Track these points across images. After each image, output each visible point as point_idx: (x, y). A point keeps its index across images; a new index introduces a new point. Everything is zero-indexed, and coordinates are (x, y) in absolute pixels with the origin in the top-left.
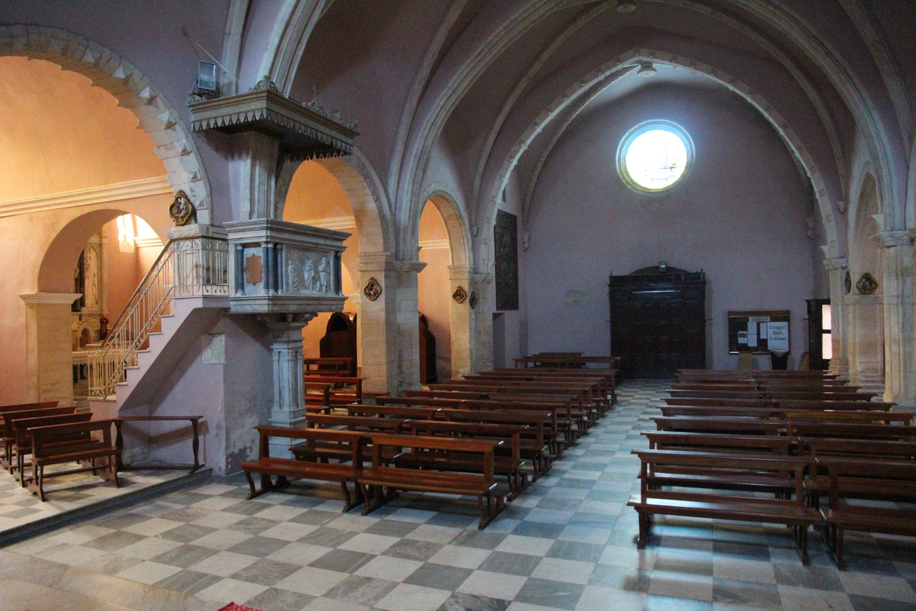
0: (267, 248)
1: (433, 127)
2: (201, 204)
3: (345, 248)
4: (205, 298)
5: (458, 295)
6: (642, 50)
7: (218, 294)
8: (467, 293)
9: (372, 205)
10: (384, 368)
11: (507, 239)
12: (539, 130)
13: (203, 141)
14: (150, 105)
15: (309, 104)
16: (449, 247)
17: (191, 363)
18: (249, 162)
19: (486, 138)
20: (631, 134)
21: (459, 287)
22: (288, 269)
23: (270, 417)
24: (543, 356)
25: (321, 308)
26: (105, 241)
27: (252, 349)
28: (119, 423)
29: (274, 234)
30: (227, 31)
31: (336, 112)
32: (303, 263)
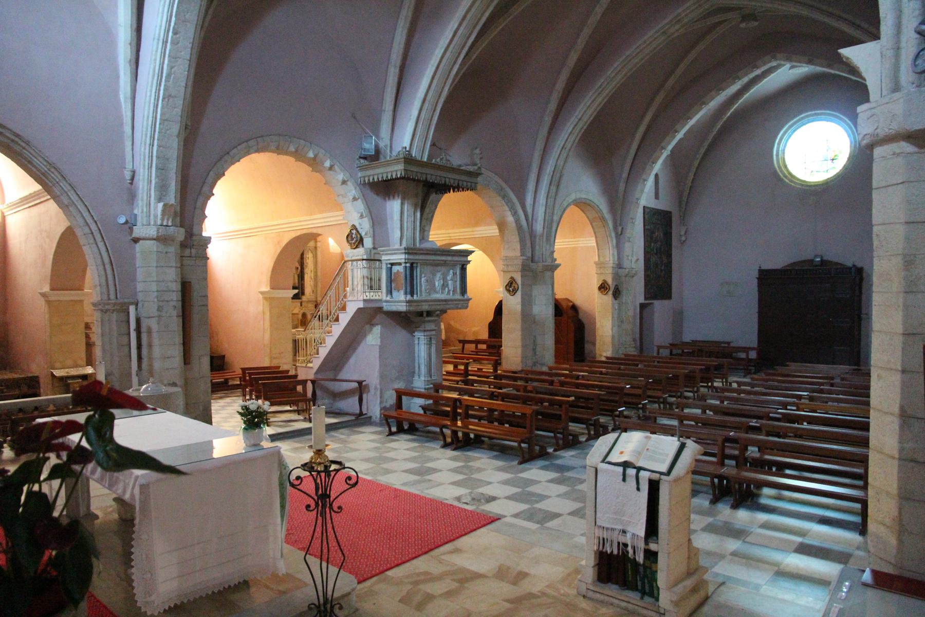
0: (406, 267)
1: (563, 150)
2: (366, 234)
3: (469, 262)
4: (365, 301)
5: (603, 287)
6: (778, 55)
7: (374, 298)
8: (611, 286)
9: (510, 219)
10: (519, 351)
11: (659, 234)
12: (680, 136)
15: (438, 160)
16: (595, 244)
17: (359, 344)
18: (399, 201)
19: (629, 147)
20: (790, 127)
21: (604, 280)
22: (422, 282)
23: (412, 383)
24: (694, 343)
25: (448, 306)
26: (319, 244)
27: (401, 334)
28: (313, 382)
29: (411, 257)
30: (383, 108)
31: (476, 148)
32: (434, 275)
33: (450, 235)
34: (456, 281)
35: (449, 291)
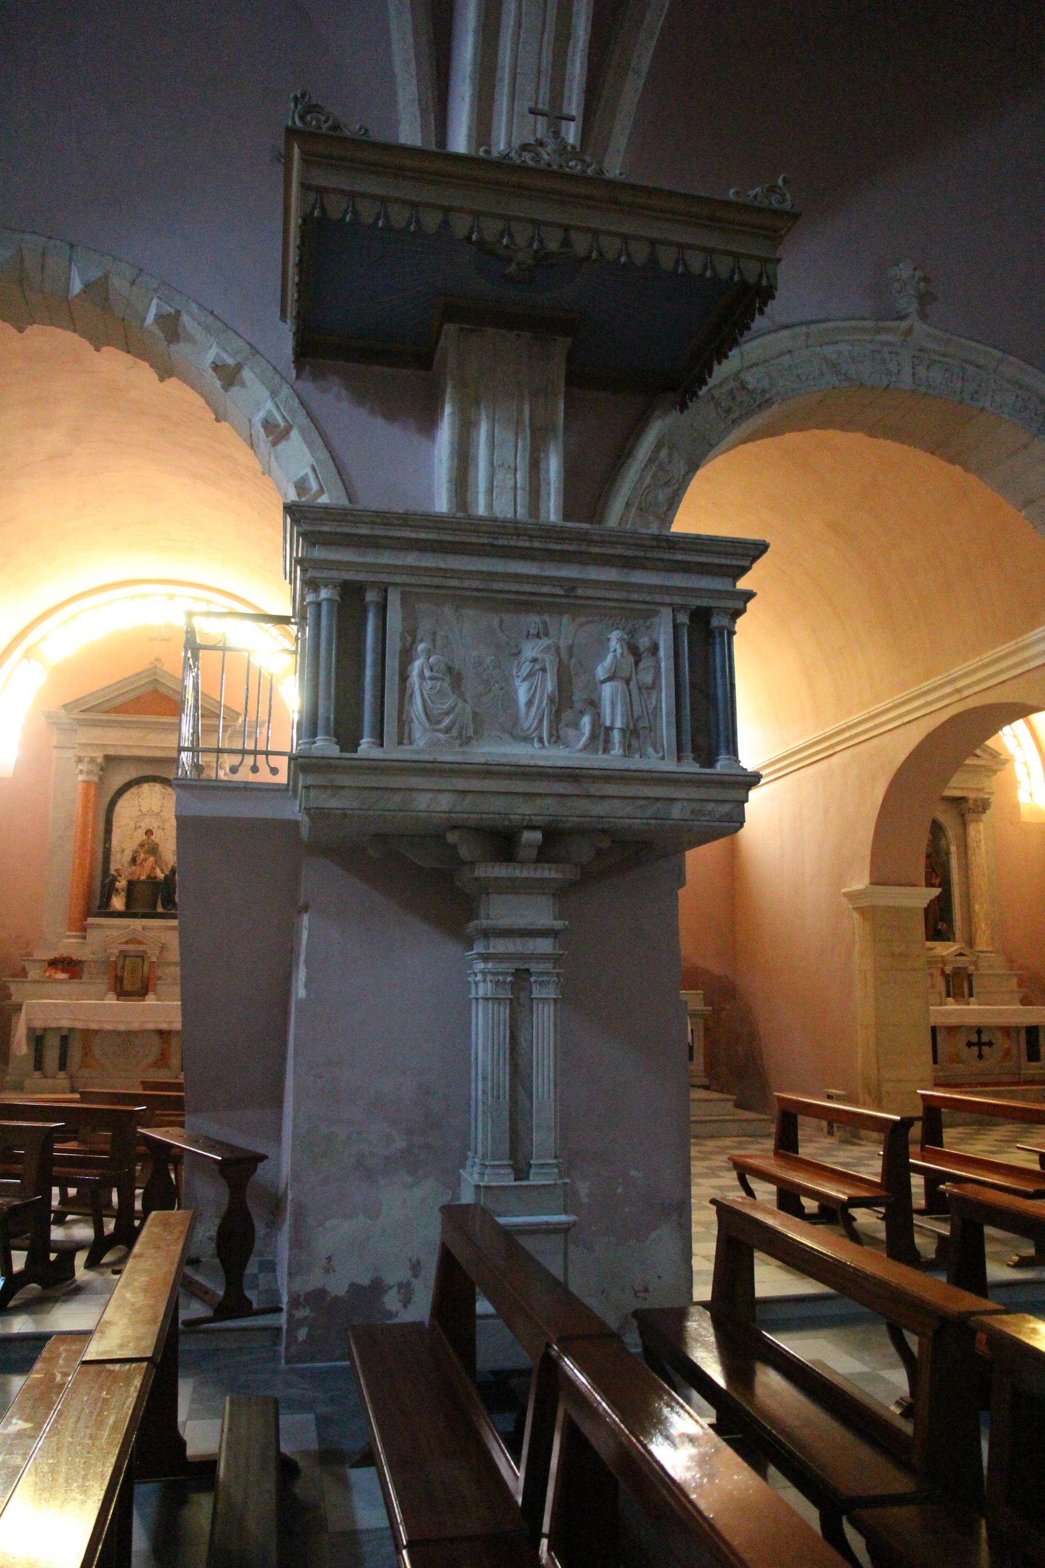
3: (749, 595)
13: (339, 398)
14: (178, 341)
33: (960, 684)
34: (655, 685)
35: (601, 736)
